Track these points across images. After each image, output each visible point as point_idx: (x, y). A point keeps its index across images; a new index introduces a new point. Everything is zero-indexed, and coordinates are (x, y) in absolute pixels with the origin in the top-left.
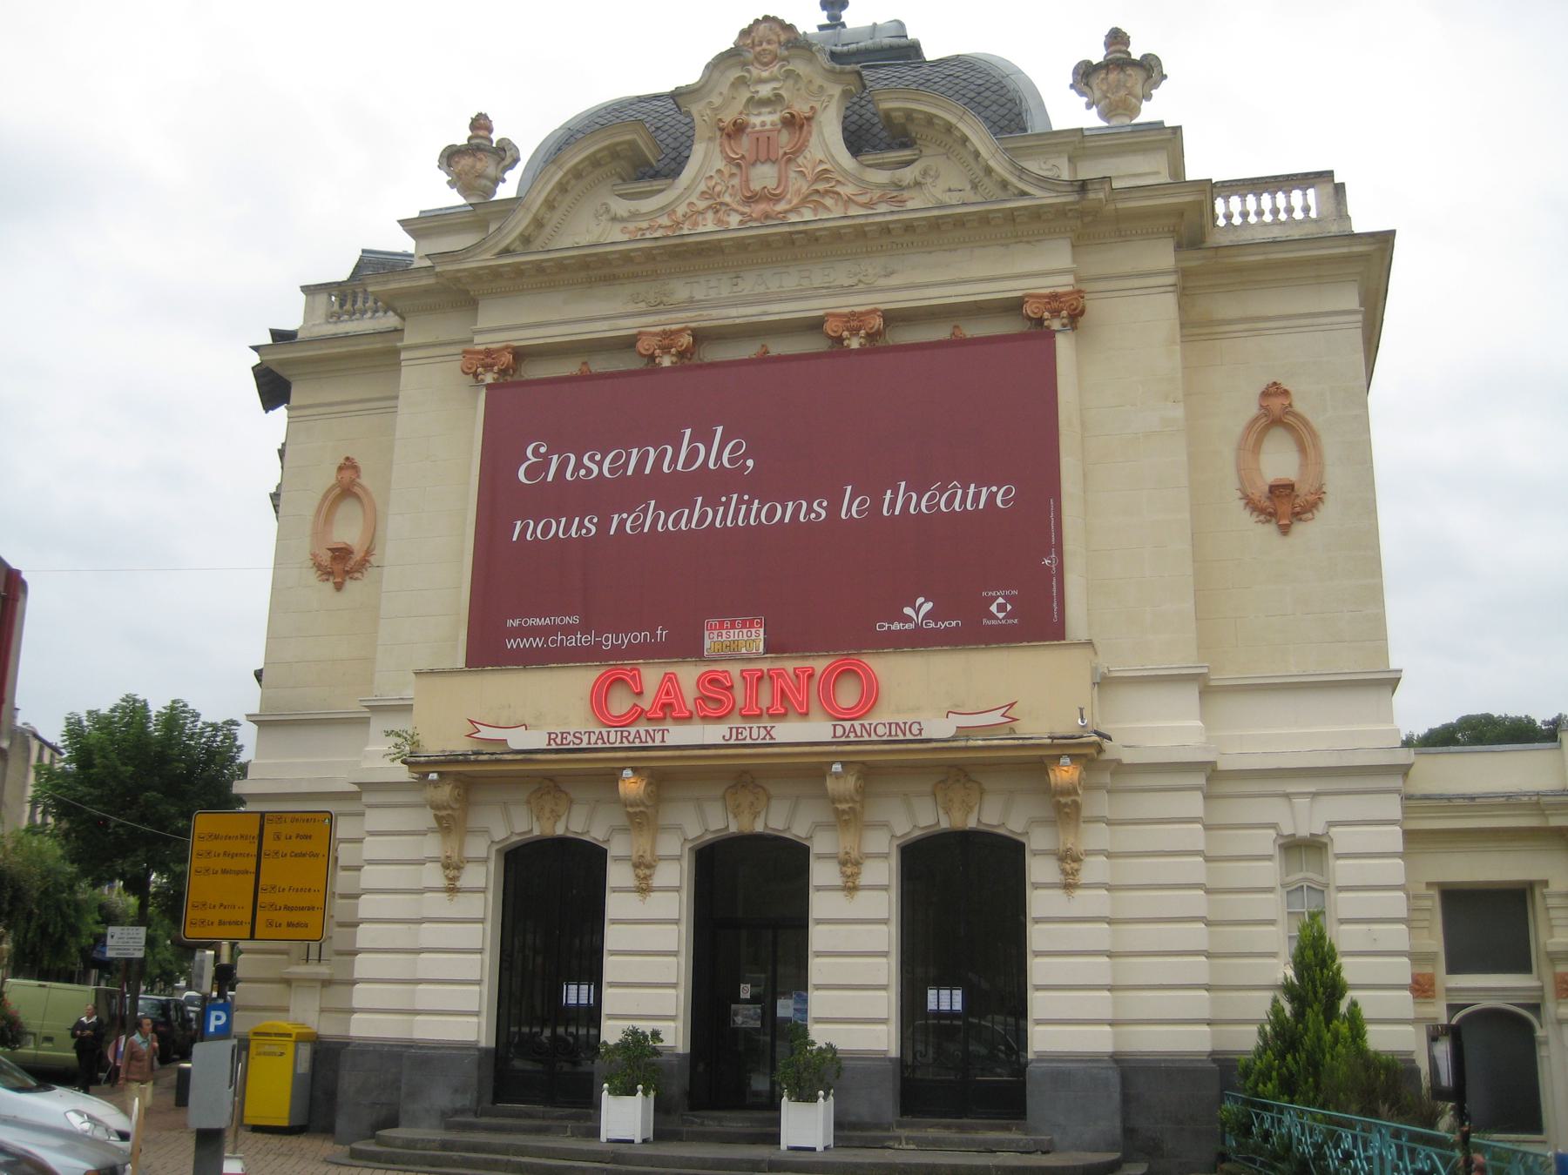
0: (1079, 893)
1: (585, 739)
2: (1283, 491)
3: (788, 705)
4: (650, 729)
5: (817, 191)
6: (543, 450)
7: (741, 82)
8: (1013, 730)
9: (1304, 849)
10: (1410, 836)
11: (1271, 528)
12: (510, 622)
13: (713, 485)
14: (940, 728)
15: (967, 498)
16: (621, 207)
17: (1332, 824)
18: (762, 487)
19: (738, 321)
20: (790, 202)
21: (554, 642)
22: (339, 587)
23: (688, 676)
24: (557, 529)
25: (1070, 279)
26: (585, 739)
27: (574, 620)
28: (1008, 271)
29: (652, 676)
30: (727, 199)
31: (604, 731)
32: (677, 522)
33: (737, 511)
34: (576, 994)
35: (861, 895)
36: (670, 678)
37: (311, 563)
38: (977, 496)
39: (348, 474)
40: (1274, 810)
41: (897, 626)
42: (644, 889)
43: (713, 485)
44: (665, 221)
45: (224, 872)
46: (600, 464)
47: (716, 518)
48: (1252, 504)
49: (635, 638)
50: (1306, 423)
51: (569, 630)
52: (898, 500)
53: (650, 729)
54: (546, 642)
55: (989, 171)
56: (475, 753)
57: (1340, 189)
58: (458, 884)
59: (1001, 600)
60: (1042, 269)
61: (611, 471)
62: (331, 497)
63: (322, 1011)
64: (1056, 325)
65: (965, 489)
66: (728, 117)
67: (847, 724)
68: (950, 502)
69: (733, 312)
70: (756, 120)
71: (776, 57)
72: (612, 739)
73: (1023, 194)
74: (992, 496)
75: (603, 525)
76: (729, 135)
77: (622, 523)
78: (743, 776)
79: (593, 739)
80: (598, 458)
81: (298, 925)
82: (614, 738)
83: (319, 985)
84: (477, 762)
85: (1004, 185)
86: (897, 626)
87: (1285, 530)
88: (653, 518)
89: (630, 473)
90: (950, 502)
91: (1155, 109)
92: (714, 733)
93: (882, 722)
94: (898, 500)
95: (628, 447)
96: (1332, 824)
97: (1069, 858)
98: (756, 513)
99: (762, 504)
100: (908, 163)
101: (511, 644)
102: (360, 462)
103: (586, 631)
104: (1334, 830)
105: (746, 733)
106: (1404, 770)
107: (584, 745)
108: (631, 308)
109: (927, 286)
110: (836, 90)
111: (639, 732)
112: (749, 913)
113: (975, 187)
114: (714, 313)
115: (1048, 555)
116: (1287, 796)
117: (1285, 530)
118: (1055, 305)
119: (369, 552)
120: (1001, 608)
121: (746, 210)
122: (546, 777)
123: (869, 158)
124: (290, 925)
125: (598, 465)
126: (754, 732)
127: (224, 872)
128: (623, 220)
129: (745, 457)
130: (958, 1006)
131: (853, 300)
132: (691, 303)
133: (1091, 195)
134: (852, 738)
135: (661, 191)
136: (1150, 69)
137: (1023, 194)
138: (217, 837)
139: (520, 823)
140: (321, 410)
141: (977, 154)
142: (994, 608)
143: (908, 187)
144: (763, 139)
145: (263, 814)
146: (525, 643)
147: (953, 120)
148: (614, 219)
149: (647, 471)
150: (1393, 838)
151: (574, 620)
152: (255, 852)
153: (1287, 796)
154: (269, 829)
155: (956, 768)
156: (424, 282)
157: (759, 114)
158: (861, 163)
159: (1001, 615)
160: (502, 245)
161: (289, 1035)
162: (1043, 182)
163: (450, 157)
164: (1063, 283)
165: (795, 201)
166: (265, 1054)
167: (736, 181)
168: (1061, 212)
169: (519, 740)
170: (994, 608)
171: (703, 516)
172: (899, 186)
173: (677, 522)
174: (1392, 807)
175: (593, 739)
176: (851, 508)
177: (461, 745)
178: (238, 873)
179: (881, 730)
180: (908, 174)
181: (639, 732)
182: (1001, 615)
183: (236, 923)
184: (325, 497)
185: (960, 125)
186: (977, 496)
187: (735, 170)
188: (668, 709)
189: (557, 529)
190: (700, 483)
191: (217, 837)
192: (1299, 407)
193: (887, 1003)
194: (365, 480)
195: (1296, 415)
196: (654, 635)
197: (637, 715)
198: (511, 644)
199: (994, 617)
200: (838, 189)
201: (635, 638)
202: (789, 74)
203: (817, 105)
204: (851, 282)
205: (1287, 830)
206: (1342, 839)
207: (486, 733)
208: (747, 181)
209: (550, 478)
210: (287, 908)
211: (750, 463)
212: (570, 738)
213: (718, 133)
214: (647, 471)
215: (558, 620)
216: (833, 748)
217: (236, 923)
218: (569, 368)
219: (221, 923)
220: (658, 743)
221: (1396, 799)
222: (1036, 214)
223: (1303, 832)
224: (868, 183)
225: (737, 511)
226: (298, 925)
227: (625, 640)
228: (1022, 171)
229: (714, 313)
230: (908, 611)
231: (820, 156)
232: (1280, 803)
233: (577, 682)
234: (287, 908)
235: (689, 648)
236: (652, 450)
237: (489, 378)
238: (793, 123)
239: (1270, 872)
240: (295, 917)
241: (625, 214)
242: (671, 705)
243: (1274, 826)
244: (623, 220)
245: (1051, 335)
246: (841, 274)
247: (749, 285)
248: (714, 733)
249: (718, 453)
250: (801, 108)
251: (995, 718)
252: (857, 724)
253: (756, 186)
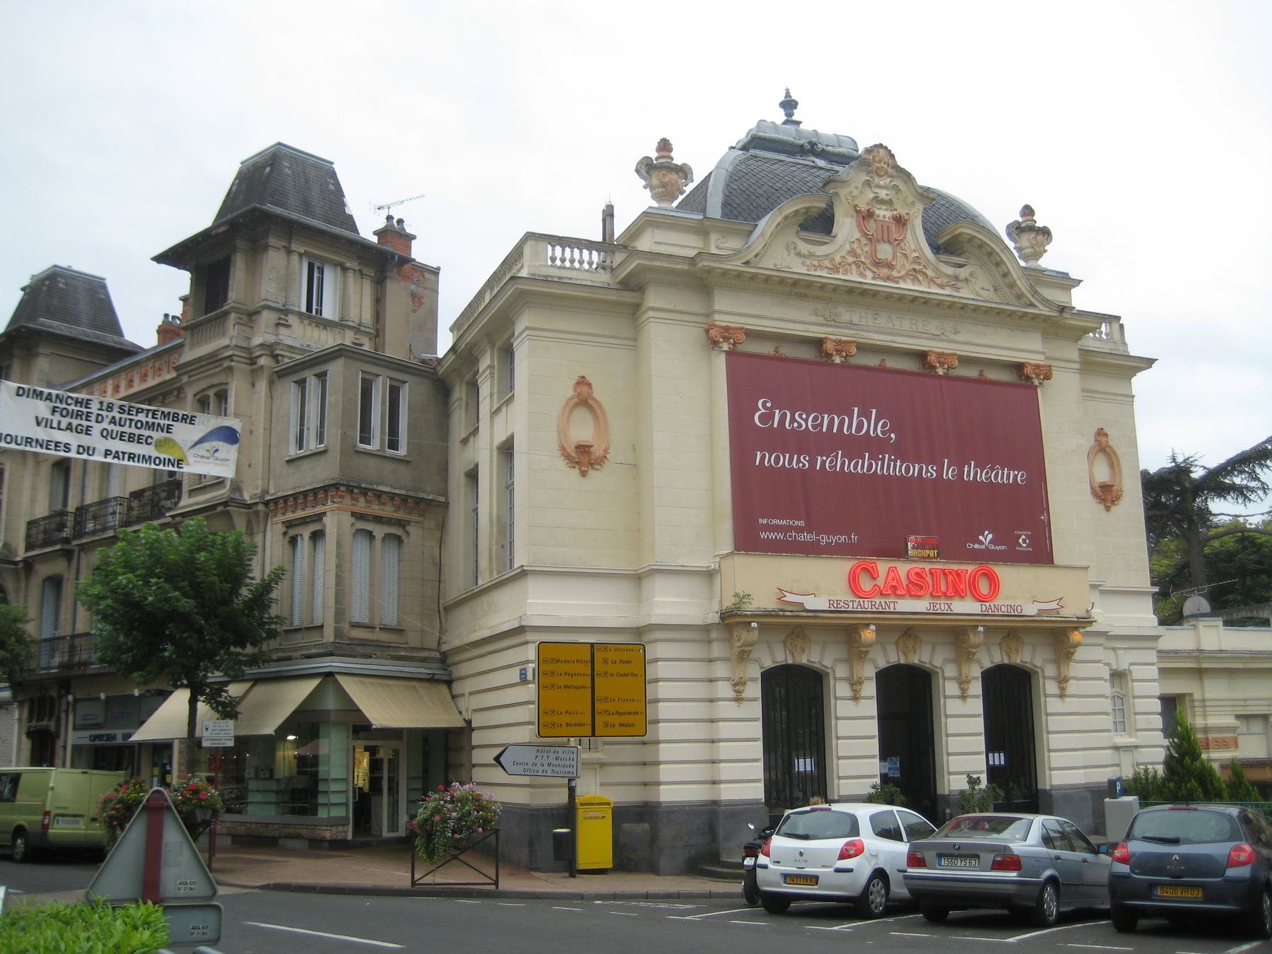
0: (1067, 699)
6: (769, 405)
7: (868, 183)
9: (1118, 676)
10: (1162, 671)
11: (1101, 507)
12: (761, 521)
13: (875, 447)
14: (1030, 610)
15: (1005, 476)
16: (804, 248)
17: (1131, 664)
18: (900, 452)
22: (584, 474)
23: (903, 568)
24: (784, 460)
25: (1041, 357)
27: (802, 523)
29: (883, 566)
32: (856, 467)
35: (969, 700)
37: (559, 453)
38: (1009, 475)
39: (585, 389)
40: (1108, 656)
41: (976, 546)
43: (875, 447)
44: (827, 263)
45: (566, 687)
46: (806, 421)
47: (877, 467)
50: (1115, 453)
51: (799, 530)
52: (971, 472)
55: (1012, 285)
57: (1122, 326)
58: (744, 695)
60: (1027, 348)
61: (814, 427)
63: (602, 785)
64: (1036, 382)
66: (863, 207)
68: (996, 477)
69: (876, 336)
70: (877, 212)
71: (886, 173)
73: (1032, 305)
74: (1016, 476)
75: (813, 463)
77: (823, 463)
78: (908, 631)
81: (627, 725)
82: (867, 605)
85: (1020, 296)
86: (976, 546)
88: (838, 462)
90: (996, 477)
94: (971, 472)
96: (1131, 664)
97: (1062, 681)
100: (961, 266)
101: (763, 535)
104: (1132, 667)
106: (1156, 638)
108: (821, 320)
110: (920, 207)
113: (996, 290)
114: (866, 334)
116: (1114, 649)
119: (606, 451)
120: (1024, 541)
122: (792, 624)
123: (944, 257)
124: (621, 725)
125: (805, 422)
126: (942, 605)
127: (566, 687)
128: (804, 256)
129: (890, 431)
132: (851, 325)
136: (1046, 232)
137: (1032, 305)
138: (558, 661)
139: (775, 655)
145: (592, 645)
146: (772, 536)
150: (1153, 672)
151: (802, 523)
153: (1114, 649)
154: (598, 656)
155: (1012, 631)
162: (1046, 302)
163: (647, 168)
165: (903, 273)
167: (867, 249)
168: (1047, 319)
169: (812, 603)
171: (870, 466)
172: (957, 278)
173: (856, 467)
174: (1152, 656)
176: (949, 473)
177: (770, 604)
178: (578, 688)
180: (963, 272)
183: (580, 725)
184: (567, 404)
186: (1009, 475)
188: (894, 590)
189: (784, 460)
191: (558, 661)
192: (1111, 443)
194: (597, 394)
196: (850, 539)
198: (763, 535)
206: (1137, 672)
207: (790, 598)
210: (617, 713)
211: (893, 436)
217: (580, 725)
218: (766, 349)
222: (1035, 317)
223: (1121, 668)
226: (627, 725)
227: (834, 539)
231: (913, 247)
232: (1111, 653)
234: (617, 713)
237: (726, 347)
238: (900, 221)
239: (1106, 688)
243: (1107, 664)
244: (804, 256)
245: (1035, 388)
246: (933, 326)
247: (882, 321)
249: (875, 427)
250: (902, 211)
251: (1053, 606)
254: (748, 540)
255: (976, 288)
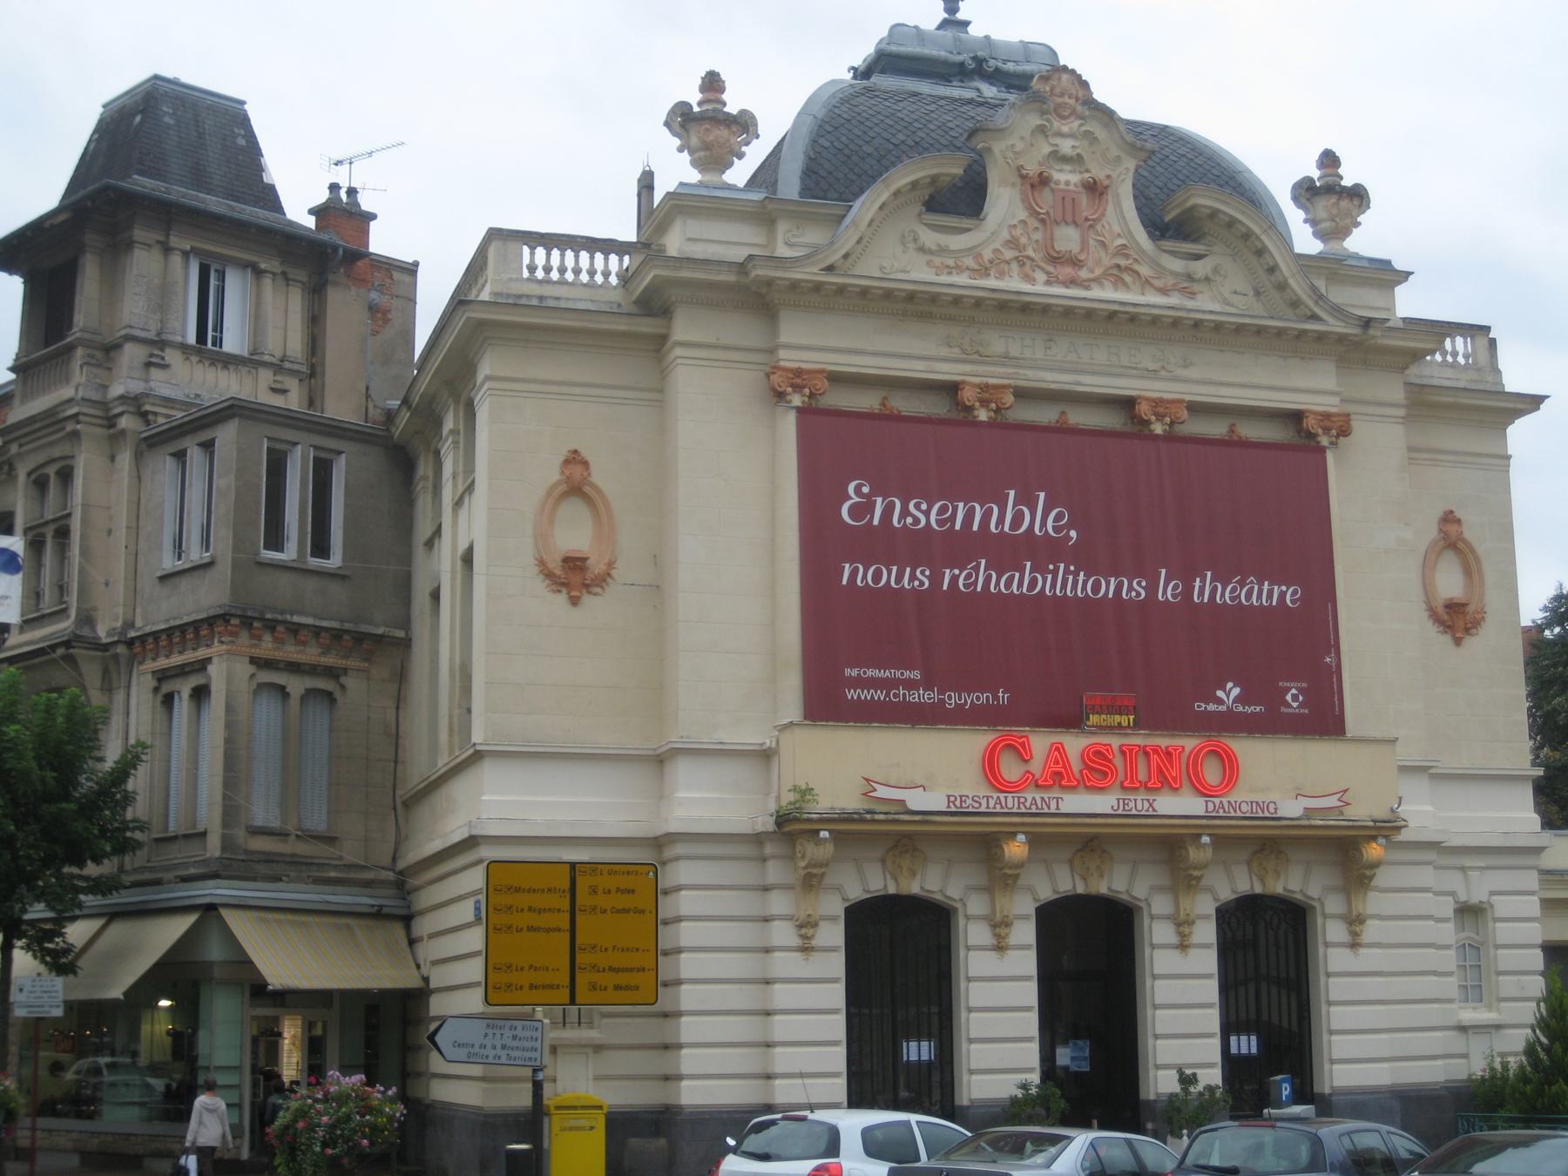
0: (1362, 951)
1: (984, 802)
2: (1454, 608)
3: (1164, 781)
4: (1046, 796)
5: (1118, 266)
6: (865, 490)
7: (1041, 130)
8: (1342, 813)
9: (1470, 913)
10: (1549, 905)
11: (1447, 638)
12: (848, 672)
13: (1044, 552)
14: (1291, 809)
15: (1263, 594)
16: (930, 238)
17: (1492, 893)
18: (1084, 559)
19: (1053, 386)
20: (1092, 271)
21: (896, 696)
22: (574, 601)
23: (1075, 744)
24: (889, 577)
25: (1335, 400)
26: (984, 802)
27: (915, 675)
28: (1486, 450)
29: (1040, 742)
30: (1030, 253)
31: (1002, 796)
32: (1008, 584)
33: (1065, 581)
34: (1246, 1045)
35: (1193, 952)
36: (1058, 748)
37: (536, 570)
38: (1270, 593)
39: (577, 470)
40: (1454, 881)
41: (1212, 707)
42: (1000, 947)
43: (1044, 552)
44: (969, 262)
45: (531, 929)
46: (927, 513)
47: (1044, 584)
48: (1434, 616)
49: (978, 698)
50: (1473, 551)
51: (910, 685)
52: (1204, 589)
53: (1046, 796)
54: (888, 695)
55: (1282, 287)
56: (868, 812)
57: (1493, 342)
58: (814, 943)
59: (1294, 691)
60: (1311, 387)
61: (940, 523)
62: (557, 493)
63: (596, 1078)
64: (1324, 441)
65: (1261, 584)
66: (1032, 168)
67: (1217, 800)
68: (1249, 595)
69: (1049, 376)
70: (1057, 176)
71: (1073, 112)
72: (1010, 804)
73: (1314, 317)
74: (1282, 595)
75: (936, 579)
76: (1033, 186)
77: (954, 579)
78: (1089, 842)
79: (992, 804)
80: (924, 507)
81: (628, 988)
82: (1011, 802)
83: (590, 1051)
84: (873, 821)
85: (1295, 304)
86: (1212, 707)
87: (1458, 642)
88: (980, 577)
89: (958, 527)
90: (1249, 595)
91: (1364, 241)
92: (1101, 803)
93: (1243, 798)
94: (1204, 589)
95: (954, 499)
96: (1492, 893)
97: (1354, 921)
98: (1079, 585)
99: (1088, 576)
100: (1198, 257)
101: (851, 694)
102: (586, 453)
103: (929, 688)
104: (1495, 898)
105: (1132, 804)
106: (1538, 851)
107: (983, 809)
108: (955, 352)
109: (1222, 384)
110: (1131, 164)
111: (1032, 798)
112: (1090, 967)
113: (1258, 293)
114: (1030, 373)
115: (1329, 653)
116: (1463, 869)
117: (1458, 642)
118: (1327, 423)
119: (611, 565)
120: (1295, 698)
121: (1050, 268)
122: (902, 836)
123: (1168, 244)
124: (617, 987)
125: (925, 515)
126: (1138, 803)
127: (531, 929)
128: (930, 252)
129: (1070, 526)
130: (1254, 1050)
131: (1158, 385)
132: (1006, 359)
133: (1371, 332)
134: (1221, 813)
135: (969, 230)
136: (1358, 196)
137: (1314, 317)
138: (518, 890)
139: (869, 880)
140: (534, 387)
141: (1272, 270)
142: (1289, 698)
143: (1199, 281)
144: (1068, 200)
145: (573, 865)
146: (866, 695)
147: (1258, 231)
148: (922, 250)
149: (975, 528)
150: (1532, 906)
151: (915, 675)
152: (567, 907)
153: (1463, 869)
154: (583, 883)
155: (1268, 842)
156: (722, 278)
157: (1061, 171)
158: (1159, 248)
159: (1295, 705)
160: (828, 262)
161: (600, 1107)
162: (1337, 311)
163: (682, 120)
164: (1330, 404)
165: (1098, 272)
166: (571, 1129)
167: (1038, 236)
168: (1341, 339)
169: (918, 801)
170: (1289, 698)
171: (1033, 582)
172: (1190, 277)
173: (1008, 584)
174: (1531, 880)
175: (992, 804)
176: (1167, 591)
177: (850, 801)
178: (548, 930)
179: (1245, 808)
180: (1201, 268)
181: (1032, 798)
182: (1295, 705)
183: (551, 987)
184: (549, 494)
185: (1263, 237)
186: (1270, 593)
187: (1036, 224)
188: (1059, 777)
189: (889, 577)
190: (1023, 546)
191: (518, 890)
192: (1467, 535)
193: (1031, 1054)
194: (597, 477)
195: (1466, 542)
196: (996, 697)
197: (1030, 781)
198: (851, 694)
199: (1289, 706)
200: (1136, 267)
201: (978, 698)
202: (1088, 135)
203: (1114, 175)
204: (1151, 366)
205: (1463, 898)
206: (1503, 906)
207: (882, 792)
208: (1052, 239)
209: (876, 522)
210: (611, 969)
211: (1073, 534)
212: (969, 802)
213: (1019, 180)
214: (975, 528)
215: (898, 674)
216: (1204, 822)
217: (551, 987)
218: (866, 401)
219: (532, 987)
220: (1053, 810)
221: (1535, 873)
222: (1321, 337)
223: (1474, 900)
224: (1164, 268)
225: (1065, 581)
226: (628, 988)
227: (969, 699)
228: (1320, 298)
229: (1030, 373)
230: (1220, 694)
231: (1117, 229)
232: (1458, 875)
233: (970, 744)
234: (611, 969)
235: (1073, 721)
236: (978, 507)
237: (797, 400)
238: (1095, 189)
239: (1448, 932)
240: (622, 979)
241: (934, 248)
242: (1060, 773)
243: (1452, 894)
244: (930, 252)
245: (1322, 450)
246: (1146, 357)
247: (1061, 350)
248: (1101, 803)
249: (1043, 520)
250: (1099, 173)
251: (1332, 802)
252: (1225, 800)
253: (1061, 246)
254: (826, 702)
255: (1223, 293)
